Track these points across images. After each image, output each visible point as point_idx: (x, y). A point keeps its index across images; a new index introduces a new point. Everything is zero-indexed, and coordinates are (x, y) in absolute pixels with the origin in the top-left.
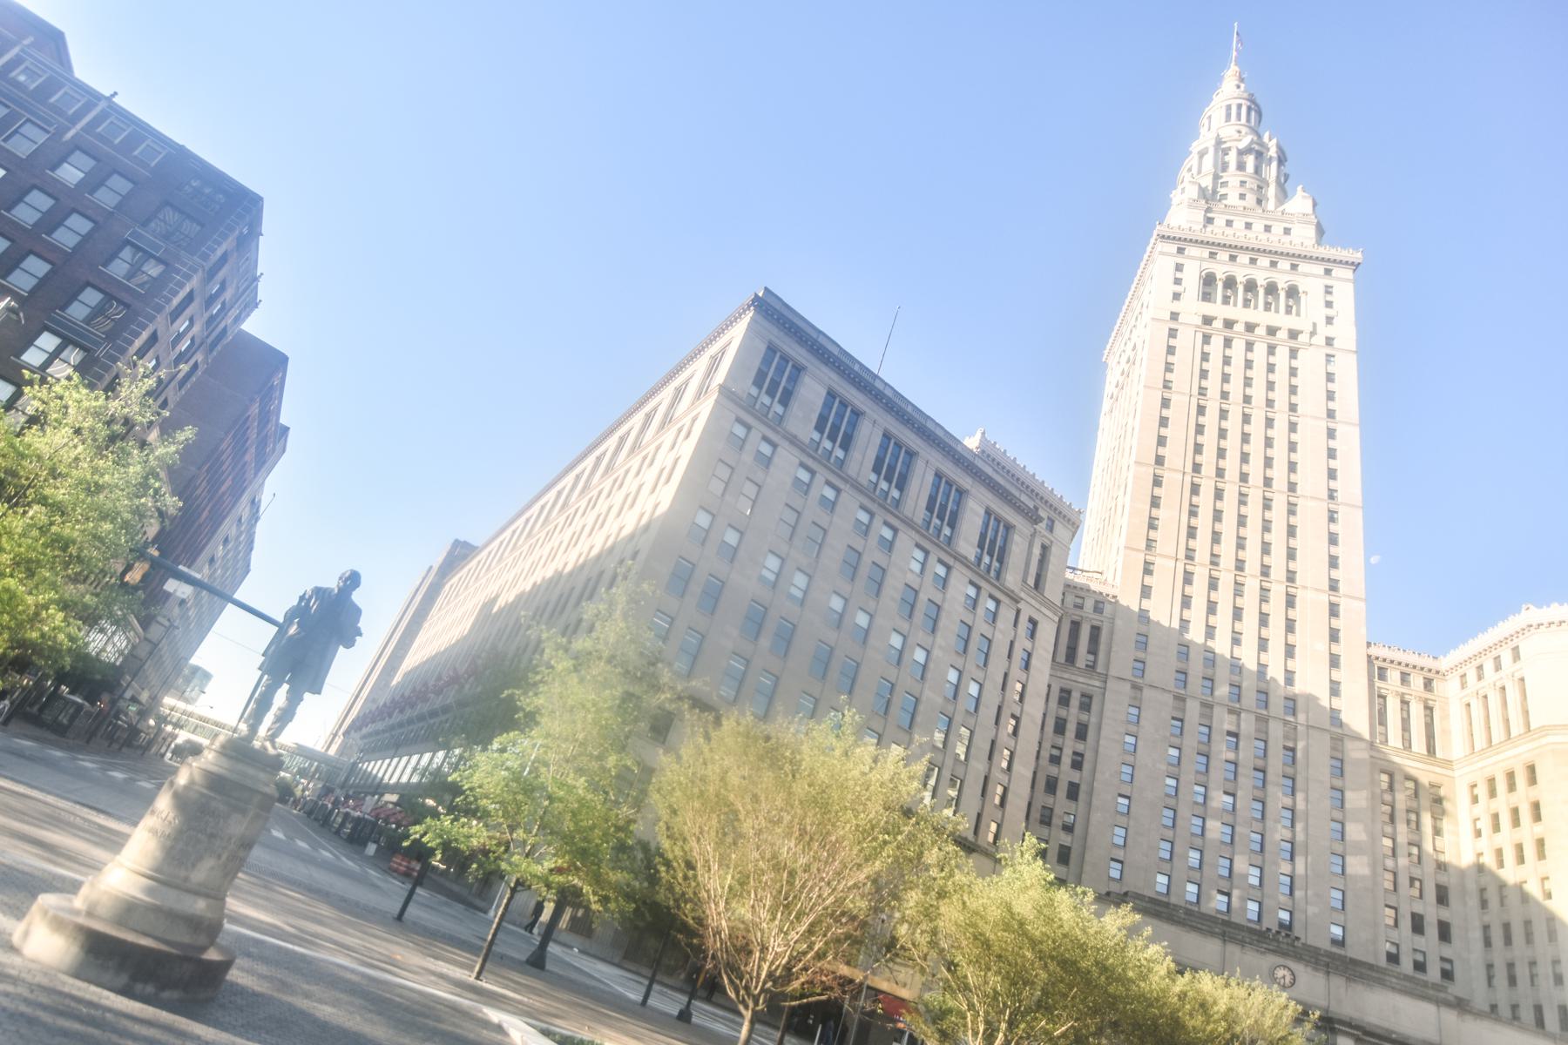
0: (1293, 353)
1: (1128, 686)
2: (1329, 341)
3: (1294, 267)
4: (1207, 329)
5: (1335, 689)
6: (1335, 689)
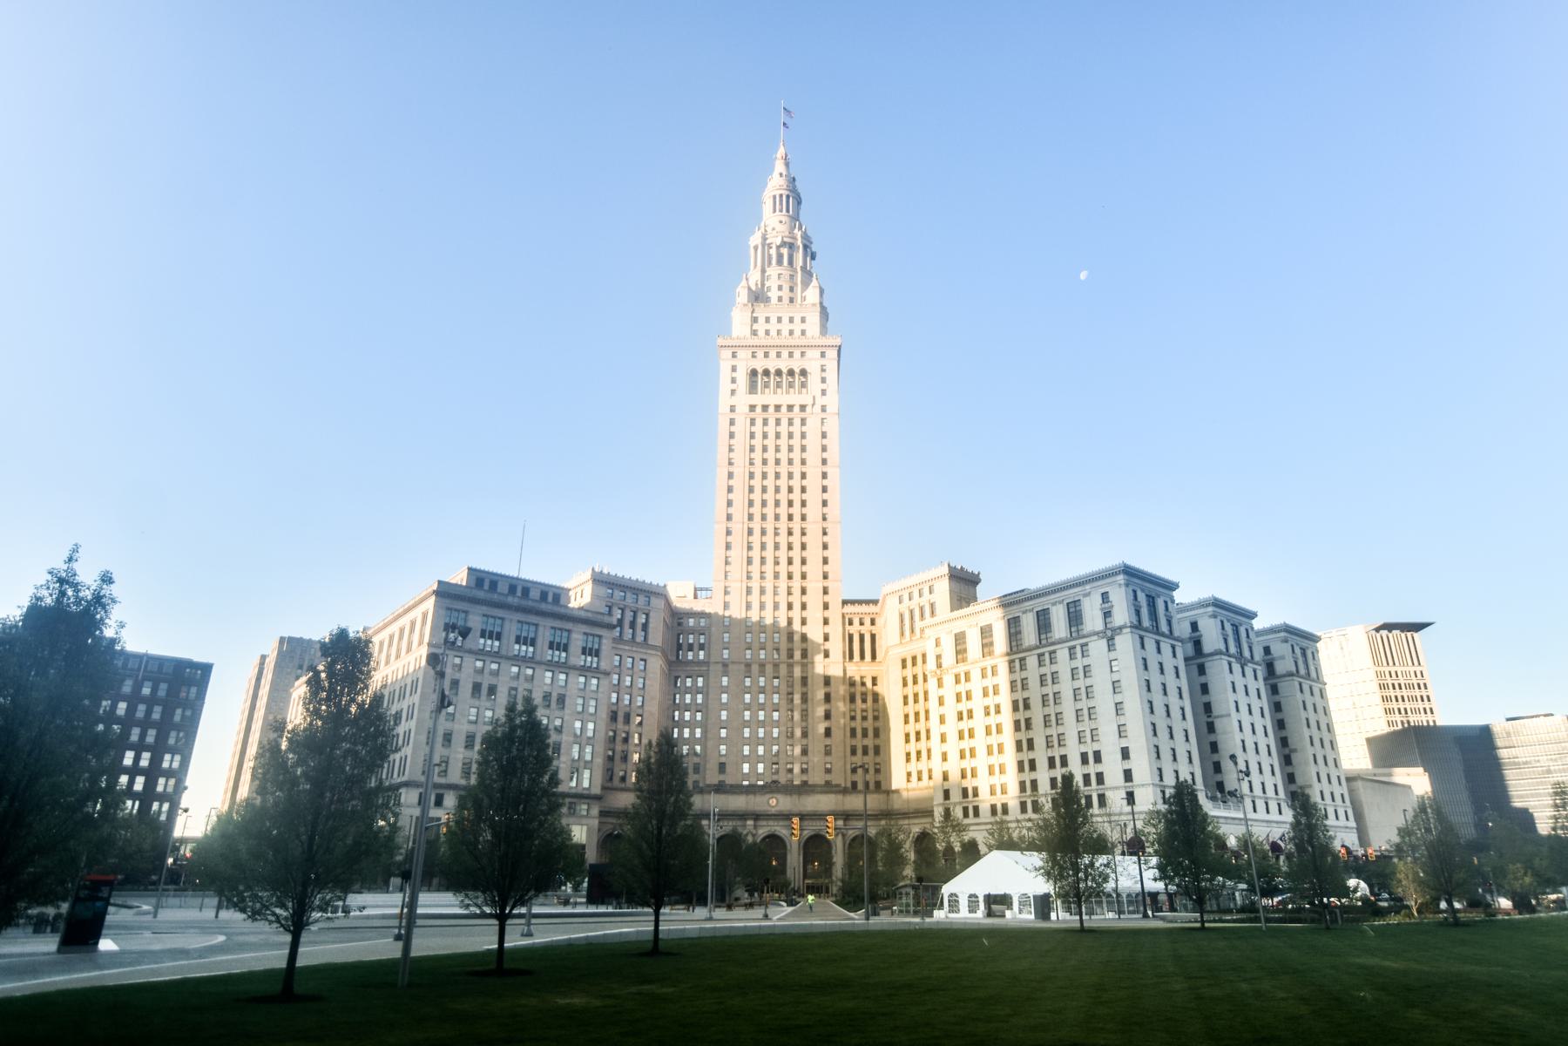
0: (803, 422)
1: (720, 667)
2: (824, 409)
3: (803, 354)
4: (753, 415)
5: (826, 638)
6: (826, 638)
